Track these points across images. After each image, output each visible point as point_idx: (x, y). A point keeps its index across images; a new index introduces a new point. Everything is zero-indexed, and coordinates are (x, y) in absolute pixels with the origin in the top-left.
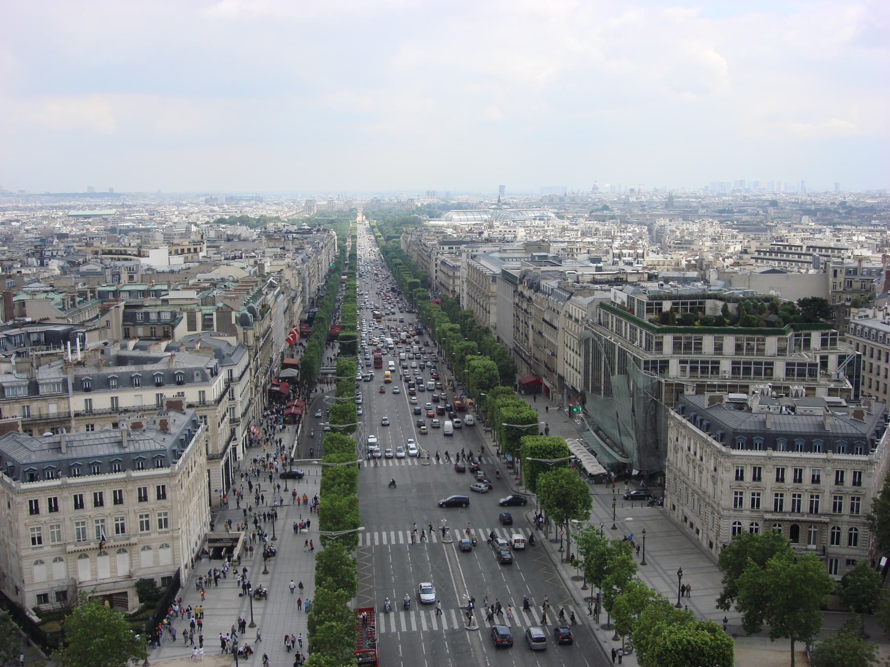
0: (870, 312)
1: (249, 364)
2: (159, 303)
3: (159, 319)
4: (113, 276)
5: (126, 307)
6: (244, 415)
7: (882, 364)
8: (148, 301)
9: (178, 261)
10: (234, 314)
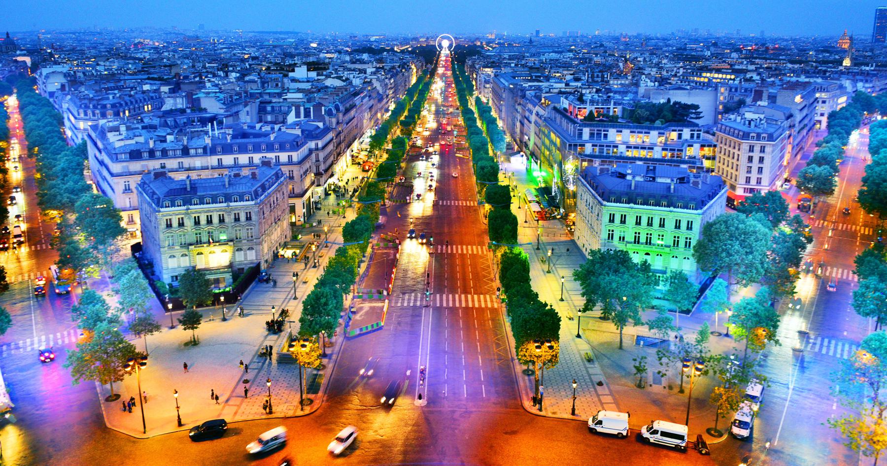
0: (732, 117)
1: (332, 140)
2: (281, 100)
3: (281, 111)
4: (263, 83)
5: (261, 102)
6: (326, 171)
7: (736, 151)
8: (274, 100)
9: (313, 75)
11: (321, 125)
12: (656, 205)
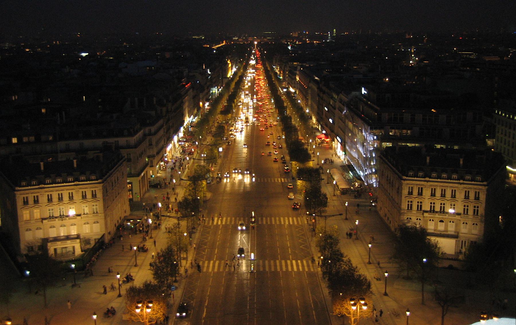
10: (155, 99)
11: (153, 113)
12: (472, 181)
